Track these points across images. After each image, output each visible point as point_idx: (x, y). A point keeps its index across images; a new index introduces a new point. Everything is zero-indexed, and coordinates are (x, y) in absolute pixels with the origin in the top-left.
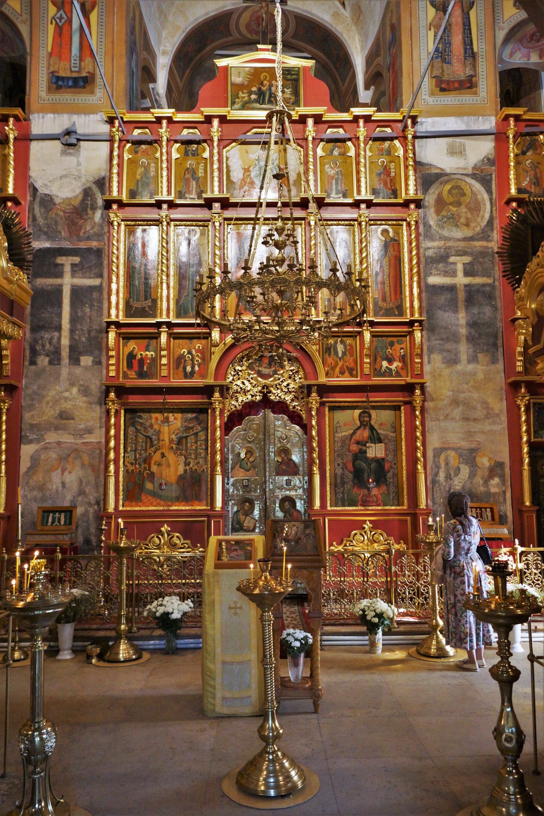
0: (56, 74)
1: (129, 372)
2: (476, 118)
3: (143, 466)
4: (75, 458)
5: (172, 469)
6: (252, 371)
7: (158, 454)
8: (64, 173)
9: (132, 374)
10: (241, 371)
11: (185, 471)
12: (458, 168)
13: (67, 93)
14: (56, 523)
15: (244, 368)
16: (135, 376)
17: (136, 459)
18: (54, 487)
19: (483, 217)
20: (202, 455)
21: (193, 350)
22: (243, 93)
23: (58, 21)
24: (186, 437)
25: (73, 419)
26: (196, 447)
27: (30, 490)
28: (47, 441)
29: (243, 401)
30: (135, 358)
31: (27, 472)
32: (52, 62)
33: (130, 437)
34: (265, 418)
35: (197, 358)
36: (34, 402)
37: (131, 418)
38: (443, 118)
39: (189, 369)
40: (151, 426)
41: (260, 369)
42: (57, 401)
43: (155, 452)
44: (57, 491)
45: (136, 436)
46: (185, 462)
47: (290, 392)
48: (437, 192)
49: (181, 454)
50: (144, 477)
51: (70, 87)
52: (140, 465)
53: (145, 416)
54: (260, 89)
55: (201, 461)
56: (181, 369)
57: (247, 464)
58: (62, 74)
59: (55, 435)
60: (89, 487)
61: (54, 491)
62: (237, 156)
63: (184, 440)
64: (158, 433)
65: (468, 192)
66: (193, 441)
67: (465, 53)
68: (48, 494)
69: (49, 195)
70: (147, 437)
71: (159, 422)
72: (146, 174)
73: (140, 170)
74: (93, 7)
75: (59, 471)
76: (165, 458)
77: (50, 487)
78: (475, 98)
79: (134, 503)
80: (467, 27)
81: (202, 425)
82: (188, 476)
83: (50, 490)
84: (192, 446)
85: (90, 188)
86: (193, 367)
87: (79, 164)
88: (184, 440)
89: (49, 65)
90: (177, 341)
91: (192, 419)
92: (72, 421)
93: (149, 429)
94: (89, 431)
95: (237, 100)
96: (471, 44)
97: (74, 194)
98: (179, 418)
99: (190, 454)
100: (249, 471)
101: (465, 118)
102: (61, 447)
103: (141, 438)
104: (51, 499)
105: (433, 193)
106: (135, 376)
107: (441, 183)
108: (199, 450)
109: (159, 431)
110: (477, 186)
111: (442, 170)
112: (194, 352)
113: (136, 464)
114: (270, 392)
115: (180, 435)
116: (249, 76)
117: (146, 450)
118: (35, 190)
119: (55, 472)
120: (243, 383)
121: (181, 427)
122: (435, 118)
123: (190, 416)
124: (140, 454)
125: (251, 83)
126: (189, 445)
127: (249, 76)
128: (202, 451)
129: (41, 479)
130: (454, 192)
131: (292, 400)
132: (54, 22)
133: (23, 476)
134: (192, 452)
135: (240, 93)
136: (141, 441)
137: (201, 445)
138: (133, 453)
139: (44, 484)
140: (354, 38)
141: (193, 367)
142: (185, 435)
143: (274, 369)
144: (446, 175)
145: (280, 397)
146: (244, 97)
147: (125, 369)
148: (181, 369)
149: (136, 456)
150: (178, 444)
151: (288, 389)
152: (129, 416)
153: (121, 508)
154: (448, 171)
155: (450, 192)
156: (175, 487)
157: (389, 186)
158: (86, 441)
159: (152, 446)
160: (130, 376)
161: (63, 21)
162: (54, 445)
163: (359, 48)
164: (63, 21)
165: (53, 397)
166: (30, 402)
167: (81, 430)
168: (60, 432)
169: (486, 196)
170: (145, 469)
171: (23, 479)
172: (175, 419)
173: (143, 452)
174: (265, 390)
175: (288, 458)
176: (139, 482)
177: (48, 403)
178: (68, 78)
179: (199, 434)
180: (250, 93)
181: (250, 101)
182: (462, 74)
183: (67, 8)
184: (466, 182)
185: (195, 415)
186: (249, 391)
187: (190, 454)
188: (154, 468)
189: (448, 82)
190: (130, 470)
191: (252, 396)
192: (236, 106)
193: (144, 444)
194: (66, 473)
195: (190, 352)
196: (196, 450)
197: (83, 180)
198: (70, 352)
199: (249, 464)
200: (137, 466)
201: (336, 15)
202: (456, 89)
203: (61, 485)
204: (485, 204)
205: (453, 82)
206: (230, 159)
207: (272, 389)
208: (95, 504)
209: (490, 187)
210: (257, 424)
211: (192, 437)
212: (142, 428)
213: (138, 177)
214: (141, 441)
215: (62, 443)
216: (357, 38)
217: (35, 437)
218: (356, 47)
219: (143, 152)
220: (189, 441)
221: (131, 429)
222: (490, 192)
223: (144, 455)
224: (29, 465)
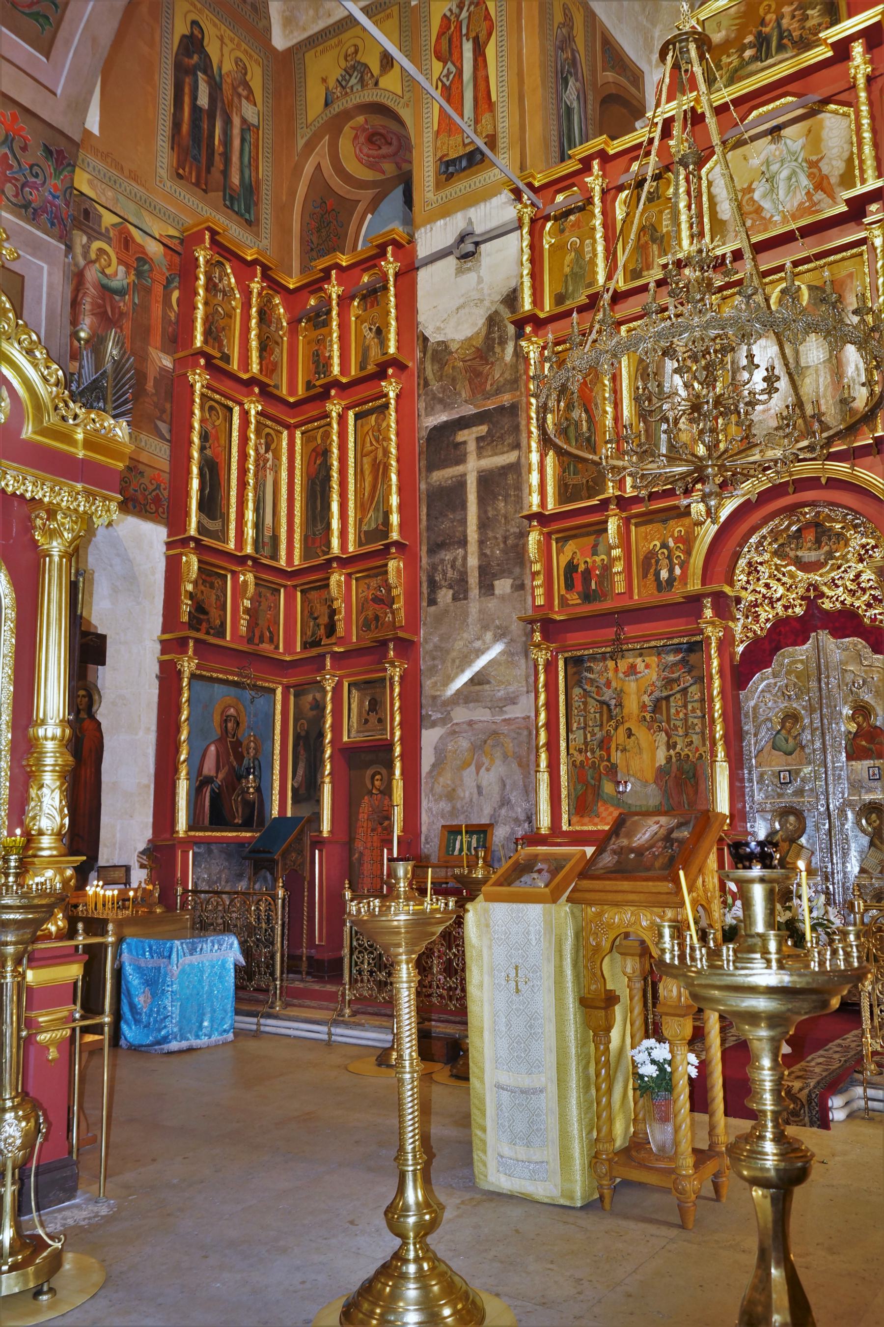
0: (446, 159)
1: (568, 596)
3: (598, 753)
4: (493, 746)
5: (646, 756)
6: (783, 560)
7: (621, 730)
8: (462, 301)
9: (574, 598)
10: (761, 564)
11: (669, 759)
13: (460, 180)
15: (767, 556)
16: (579, 601)
17: (586, 743)
18: (467, 794)
20: (698, 729)
21: (670, 540)
22: (729, 56)
23: (445, 80)
24: (667, 698)
25: (488, 682)
26: (686, 714)
27: (436, 800)
29: (768, 620)
30: (577, 571)
31: (430, 772)
32: (439, 143)
33: (576, 704)
34: (818, 648)
35: (678, 553)
36: (436, 662)
37: (575, 673)
39: (664, 574)
40: (608, 684)
41: (799, 553)
42: (466, 657)
43: (616, 729)
44: (471, 800)
45: (585, 704)
46: (668, 741)
47: (864, 590)
49: (660, 729)
50: (600, 773)
51: (465, 169)
52: (593, 752)
53: (598, 667)
55: (696, 739)
56: (651, 576)
57: (787, 741)
58: (453, 155)
59: (465, 710)
60: (514, 794)
61: (467, 800)
63: (664, 703)
64: (620, 694)
66: (680, 703)
68: (459, 806)
69: (443, 342)
70: (602, 703)
71: (621, 675)
72: (577, 260)
73: (570, 257)
74: (489, 35)
75: (473, 768)
76: (633, 738)
79: (586, 820)
81: (693, 674)
82: (674, 769)
83: (462, 799)
84: (678, 712)
85: (496, 312)
86: (671, 571)
87: (480, 280)
88: (664, 703)
89: (436, 149)
90: (642, 529)
91: (675, 664)
92: (487, 687)
93: (605, 689)
94: (512, 700)
97: (476, 329)
98: (654, 665)
99: (676, 728)
100: (790, 754)
103: (592, 705)
106: (579, 601)
108: (690, 720)
109: (622, 691)
112: (671, 543)
113: (586, 751)
114: (822, 595)
115: (657, 694)
116: (738, 21)
117: (601, 725)
118: (426, 339)
120: (767, 586)
121: (658, 679)
123: (672, 658)
124: (593, 734)
125: (741, 32)
126: (673, 711)
127: (738, 21)
128: (696, 721)
129: (449, 782)
131: (869, 605)
132: (440, 84)
134: (679, 723)
136: (592, 711)
137: (693, 711)
138: (582, 731)
139: (454, 790)
141: (671, 571)
142: (665, 694)
143: (826, 548)
145: (842, 602)
146: (731, 63)
147: (563, 592)
148: (651, 576)
149: (585, 738)
150: (654, 712)
151: (859, 584)
152: (571, 671)
153: (565, 827)
156: (652, 789)
158: (507, 717)
159: (610, 718)
160: (571, 602)
161: (451, 77)
162: (465, 726)
164: (451, 77)
166: (430, 663)
167: (500, 699)
168: (471, 705)
170: (601, 757)
172: (647, 666)
173: (596, 729)
174: (812, 594)
175: (869, 725)
176: (593, 782)
177: (453, 661)
178: (460, 158)
179: (690, 690)
180: (743, 48)
181: (743, 64)
183: (455, 56)
185: (681, 656)
186: (779, 600)
187: (676, 728)
188: (617, 757)
190: (578, 763)
191: (786, 608)
193: (598, 715)
194: (483, 769)
195: (664, 545)
196: (686, 720)
197: (487, 303)
198: (480, 576)
199: (791, 740)
200: (589, 754)
207: (825, 589)
208: (525, 821)
210: (802, 661)
211: (678, 696)
212: (594, 689)
213: (567, 270)
214: (592, 711)
215: (476, 723)
217: (439, 716)
219: (572, 226)
220: (672, 704)
221: (577, 691)
223: (599, 736)
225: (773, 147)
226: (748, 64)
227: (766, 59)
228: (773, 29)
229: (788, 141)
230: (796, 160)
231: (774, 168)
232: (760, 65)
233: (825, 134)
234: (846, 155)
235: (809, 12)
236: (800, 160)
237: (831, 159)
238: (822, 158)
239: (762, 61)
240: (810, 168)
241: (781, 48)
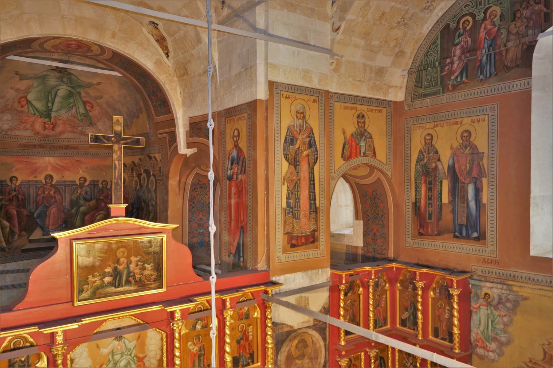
2: (317, 270)
12: (303, 323)
19: (320, 363)
22: (94, 277)
38: (293, 274)
48: (287, 350)
54: (115, 269)
62: (85, 354)
65: (309, 343)
67: (310, 208)
78: (316, 252)
80: (312, 182)
95: (86, 286)
96: (315, 199)
101: (309, 272)
105: (284, 351)
107: (290, 341)
110: (316, 335)
111: (291, 327)
116: (102, 255)
122: (286, 275)
125: (104, 262)
127: (102, 255)
130: (300, 346)
135: (90, 277)
140: (175, 89)
144: (295, 331)
146: (95, 282)
154: (296, 327)
155: (297, 347)
157: (248, 351)
163: (180, 100)
169: (322, 344)
180: (104, 275)
181: (103, 286)
182: (307, 228)
184: (308, 334)
189: (297, 238)
192: (85, 295)
201: (158, 63)
202: (303, 244)
204: (321, 351)
205: (301, 237)
206: (75, 362)
209: (325, 334)
216: (178, 89)
218: (178, 99)
222: (324, 339)
225: (116, 343)
226: (106, 286)
227: (118, 287)
228: (124, 268)
229: (126, 341)
230: (130, 355)
231: (117, 357)
232: (114, 289)
233: (148, 341)
234: (158, 357)
235: (146, 265)
236: (133, 355)
237: (150, 358)
238: (146, 356)
239: (116, 288)
240: (138, 362)
241: (128, 282)
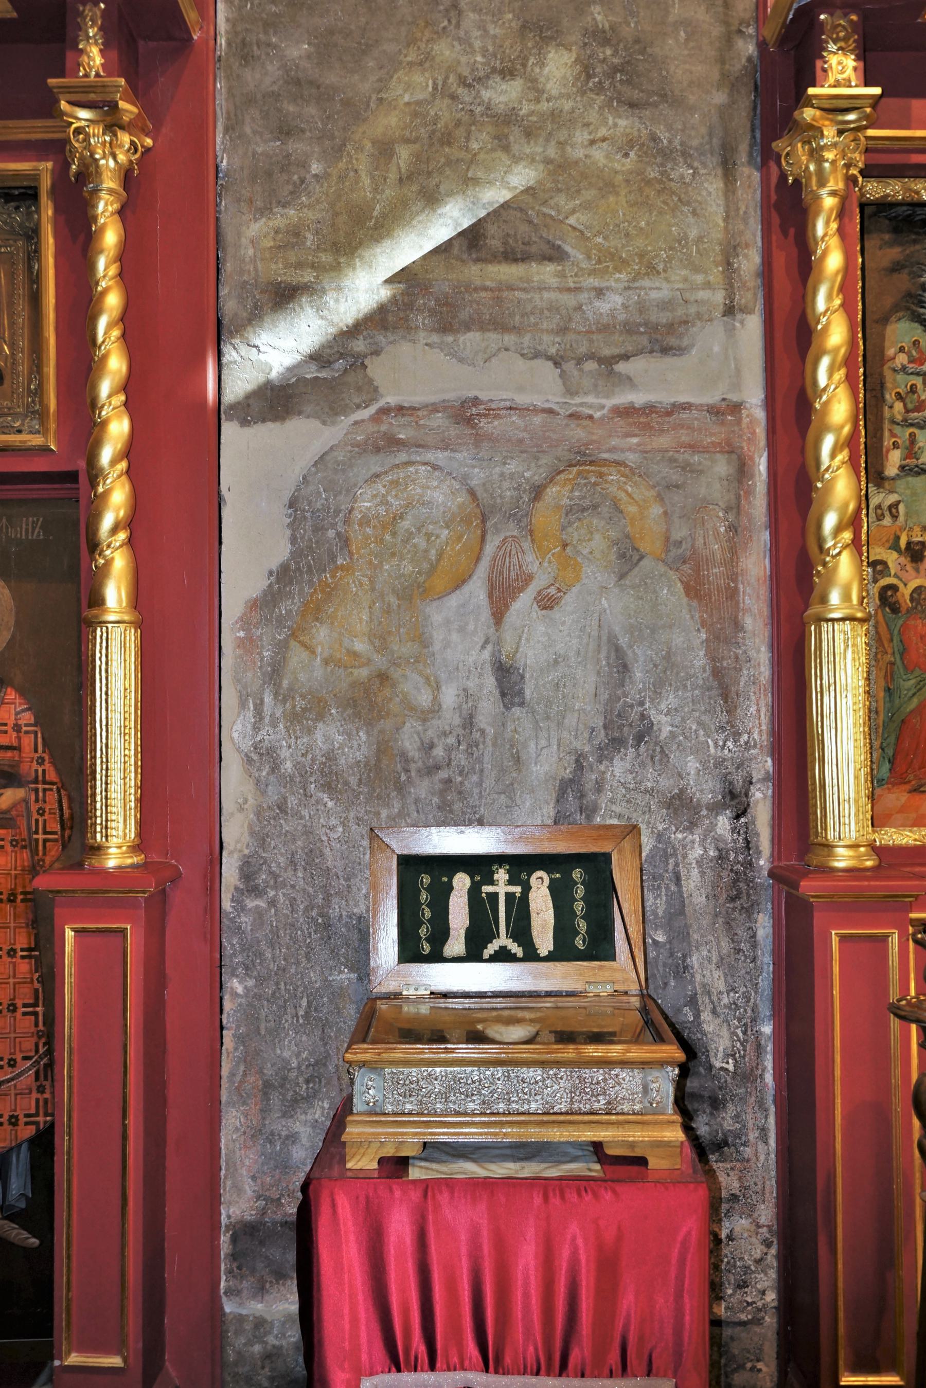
4: (575, 511)
14: (503, 940)
18: (449, 696)
25: (554, 255)
27: (294, 718)
28: (391, 399)
36: (296, 147)
37: (896, 268)
42: (447, 139)
44: (469, 722)
59: (437, 356)
60: (670, 700)
61: (450, 718)
68: (409, 742)
77: (424, 699)
83: (427, 715)
92: (546, 273)
102: (479, 439)
104: (431, 770)
119: (453, 601)
129: (360, 646)
133: (244, 622)
139: (383, 677)
158: (638, 398)
162: (439, 420)
165: (416, 111)
166: (266, 146)
167: (605, 329)
168: (471, 339)
171: (247, 644)
190: (905, 592)
194: (524, 601)
203: (490, 682)
208: (715, 808)
215: (491, 413)
224: (281, 552)
